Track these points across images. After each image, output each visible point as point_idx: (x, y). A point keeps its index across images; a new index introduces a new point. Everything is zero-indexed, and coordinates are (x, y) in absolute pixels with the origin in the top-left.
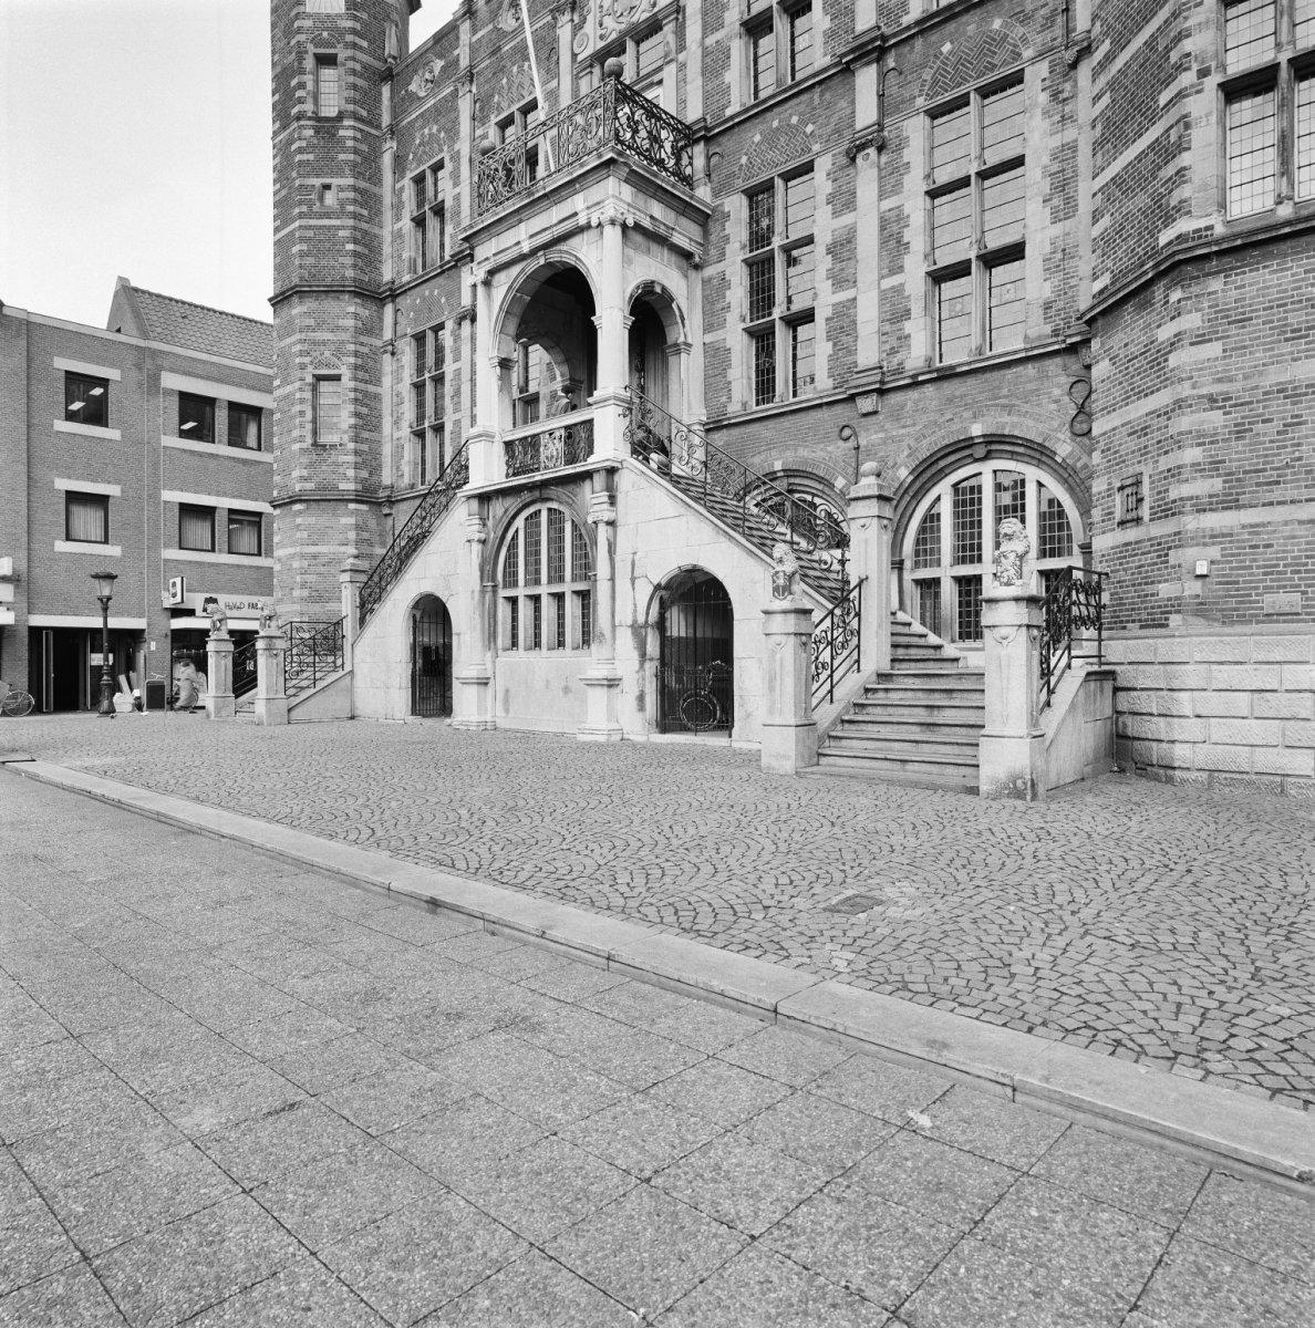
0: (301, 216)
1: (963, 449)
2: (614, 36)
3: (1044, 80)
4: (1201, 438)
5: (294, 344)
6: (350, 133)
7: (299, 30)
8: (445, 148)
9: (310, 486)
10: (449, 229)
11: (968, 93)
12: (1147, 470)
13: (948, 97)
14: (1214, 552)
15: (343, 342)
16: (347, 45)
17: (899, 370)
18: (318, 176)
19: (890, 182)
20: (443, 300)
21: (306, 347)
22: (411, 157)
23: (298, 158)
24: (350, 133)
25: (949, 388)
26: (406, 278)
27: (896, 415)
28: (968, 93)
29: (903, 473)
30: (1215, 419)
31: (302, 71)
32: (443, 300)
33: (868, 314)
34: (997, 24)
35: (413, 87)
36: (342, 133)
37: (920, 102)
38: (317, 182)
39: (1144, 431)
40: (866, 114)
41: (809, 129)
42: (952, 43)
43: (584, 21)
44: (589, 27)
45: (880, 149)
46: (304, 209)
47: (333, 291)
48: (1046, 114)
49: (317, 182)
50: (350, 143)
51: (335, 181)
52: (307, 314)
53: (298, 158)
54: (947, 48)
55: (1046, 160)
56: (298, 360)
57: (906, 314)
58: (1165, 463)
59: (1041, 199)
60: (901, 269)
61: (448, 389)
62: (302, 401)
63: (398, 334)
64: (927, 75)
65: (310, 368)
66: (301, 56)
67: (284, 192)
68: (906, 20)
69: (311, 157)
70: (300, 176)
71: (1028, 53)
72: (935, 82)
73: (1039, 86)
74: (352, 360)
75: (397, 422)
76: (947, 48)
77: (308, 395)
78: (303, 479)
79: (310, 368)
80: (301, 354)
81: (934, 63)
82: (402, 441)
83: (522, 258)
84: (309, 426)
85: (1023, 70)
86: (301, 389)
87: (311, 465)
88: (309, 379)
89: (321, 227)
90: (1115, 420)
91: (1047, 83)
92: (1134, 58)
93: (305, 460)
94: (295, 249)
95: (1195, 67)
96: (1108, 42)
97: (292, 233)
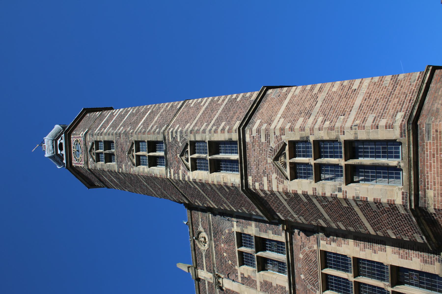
3: (327, 243)
11: (322, 273)
28: (322, 273)
34: (301, 256)
42: (301, 274)
48: (339, 245)
54: (302, 277)
55: (358, 249)
59: (374, 254)
64: (310, 287)
68: (287, 289)
72: (313, 285)
73: (328, 246)
76: (302, 277)
81: (306, 283)
85: (320, 250)
91: (328, 242)
92: (327, 212)
95: (337, 193)
96: (319, 220)
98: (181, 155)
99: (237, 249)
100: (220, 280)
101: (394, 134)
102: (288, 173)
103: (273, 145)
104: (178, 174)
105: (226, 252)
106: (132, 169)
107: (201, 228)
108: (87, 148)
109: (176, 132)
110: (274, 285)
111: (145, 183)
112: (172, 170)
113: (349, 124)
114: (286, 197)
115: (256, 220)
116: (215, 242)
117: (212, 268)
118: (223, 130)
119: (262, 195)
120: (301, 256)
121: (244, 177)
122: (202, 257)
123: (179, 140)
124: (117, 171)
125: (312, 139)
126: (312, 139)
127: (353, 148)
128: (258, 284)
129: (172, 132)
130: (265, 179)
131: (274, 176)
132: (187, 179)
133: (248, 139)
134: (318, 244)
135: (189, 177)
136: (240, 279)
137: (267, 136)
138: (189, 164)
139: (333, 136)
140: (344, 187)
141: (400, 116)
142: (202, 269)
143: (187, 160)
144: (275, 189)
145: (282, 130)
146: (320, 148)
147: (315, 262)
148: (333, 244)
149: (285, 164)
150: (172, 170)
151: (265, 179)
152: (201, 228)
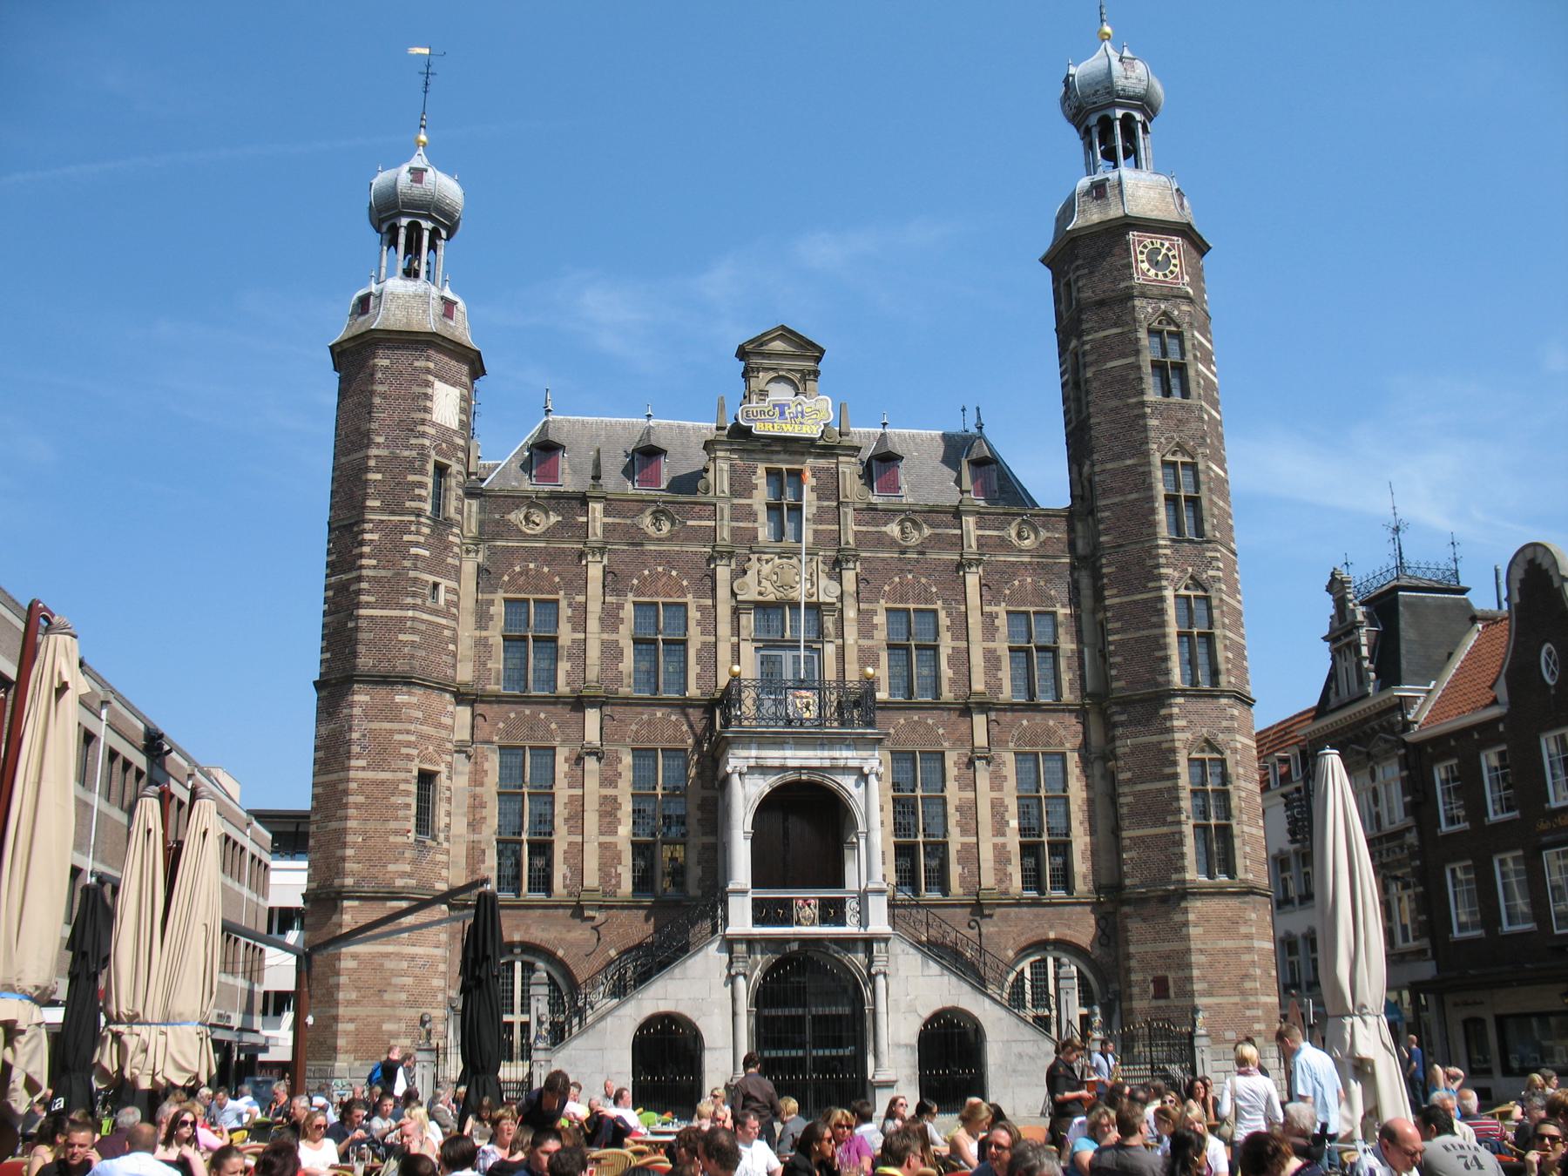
0: (414, 607)
1: (1041, 945)
2: (771, 598)
4: (1201, 966)
5: (400, 732)
6: (457, 540)
7: (423, 435)
8: (562, 593)
9: (413, 882)
10: (564, 667)
12: (1171, 976)
13: (1027, 749)
14: (1207, 1014)
15: (443, 739)
16: (459, 461)
17: (1006, 893)
18: (431, 573)
19: (997, 781)
20: (553, 726)
21: (413, 738)
22: (506, 578)
23: (413, 550)
24: (457, 540)
25: (1035, 910)
26: (493, 687)
27: (1005, 918)
29: (1011, 953)
30: (1202, 959)
31: (422, 471)
32: (553, 726)
33: (987, 854)
35: (517, 517)
36: (451, 538)
37: (1011, 745)
38: (431, 579)
39: (1168, 957)
40: (981, 739)
41: (941, 731)
43: (745, 572)
44: (751, 577)
45: (988, 763)
46: (419, 601)
47: (442, 688)
49: (431, 579)
50: (456, 550)
51: (444, 583)
52: (418, 707)
53: (413, 550)
56: (404, 751)
57: (1009, 861)
58: (1181, 974)
60: (1004, 835)
61: (560, 811)
62: (407, 793)
63: (479, 735)
65: (417, 761)
66: (424, 457)
67: (383, 573)
69: (427, 553)
70: (416, 568)
71: (1068, 745)
74: (448, 758)
75: (474, 825)
77: (413, 788)
78: (403, 875)
79: (417, 761)
80: (409, 744)
82: (483, 846)
83: (784, 769)
84: (413, 820)
86: (407, 781)
87: (413, 862)
88: (416, 773)
89: (430, 623)
90: (1149, 947)
93: (408, 854)
94: (401, 637)
97: (402, 619)
98: (1192, 577)
99: (1032, 609)
100: (974, 569)
101: (1241, 874)
102: (1195, 755)
103: (1221, 736)
104: (1167, 566)
105: (1021, 585)
106: (1155, 446)
107: (1043, 534)
108: (1166, 298)
109: (1218, 569)
110: (1000, 674)
111: (1129, 462)
112: (1168, 551)
113: (1246, 829)
114: (1165, 746)
115: (1080, 653)
116: (1030, 563)
117: (985, 549)
118: (1227, 660)
119: (1163, 712)
120: (1051, 723)
121: (1182, 693)
122: (997, 529)
123: (1211, 573)
124: (1146, 398)
125: (1230, 787)
126: (1230, 787)
127: (1225, 833)
128: (991, 645)
129: (1216, 559)
130: (1183, 723)
131: (1188, 735)
132: (1164, 583)
133: (1224, 701)
134: (1073, 750)
135: (1165, 588)
136: (987, 609)
137: (1229, 730)
138: (1182, 592)
139: (1235, 812)
140: (1191, 822)
141: (1250, 876)
142: (979, 527)
143: (1187, 588)
144: (1177, 736)
145: (1235, 751)
146: (1224, 796)
147: (1048, 744)
148: (1077, 771)
149: (1203, 751)
150: (1168, 551)
151: (1183, 723)
152: (1043, 534)
